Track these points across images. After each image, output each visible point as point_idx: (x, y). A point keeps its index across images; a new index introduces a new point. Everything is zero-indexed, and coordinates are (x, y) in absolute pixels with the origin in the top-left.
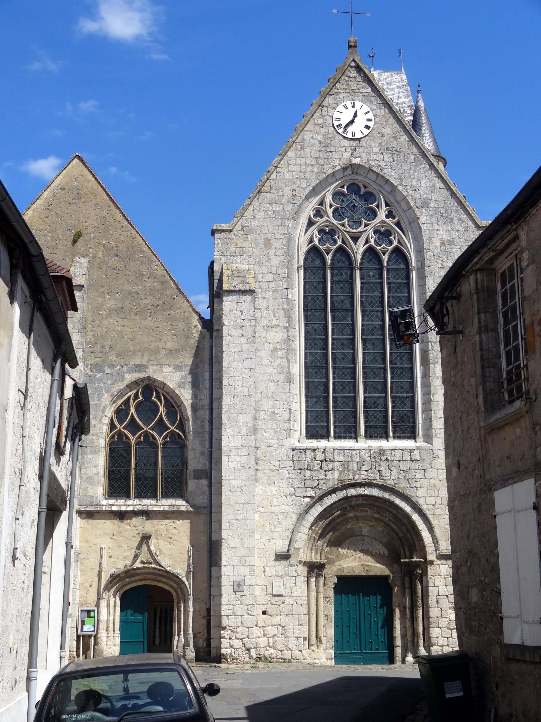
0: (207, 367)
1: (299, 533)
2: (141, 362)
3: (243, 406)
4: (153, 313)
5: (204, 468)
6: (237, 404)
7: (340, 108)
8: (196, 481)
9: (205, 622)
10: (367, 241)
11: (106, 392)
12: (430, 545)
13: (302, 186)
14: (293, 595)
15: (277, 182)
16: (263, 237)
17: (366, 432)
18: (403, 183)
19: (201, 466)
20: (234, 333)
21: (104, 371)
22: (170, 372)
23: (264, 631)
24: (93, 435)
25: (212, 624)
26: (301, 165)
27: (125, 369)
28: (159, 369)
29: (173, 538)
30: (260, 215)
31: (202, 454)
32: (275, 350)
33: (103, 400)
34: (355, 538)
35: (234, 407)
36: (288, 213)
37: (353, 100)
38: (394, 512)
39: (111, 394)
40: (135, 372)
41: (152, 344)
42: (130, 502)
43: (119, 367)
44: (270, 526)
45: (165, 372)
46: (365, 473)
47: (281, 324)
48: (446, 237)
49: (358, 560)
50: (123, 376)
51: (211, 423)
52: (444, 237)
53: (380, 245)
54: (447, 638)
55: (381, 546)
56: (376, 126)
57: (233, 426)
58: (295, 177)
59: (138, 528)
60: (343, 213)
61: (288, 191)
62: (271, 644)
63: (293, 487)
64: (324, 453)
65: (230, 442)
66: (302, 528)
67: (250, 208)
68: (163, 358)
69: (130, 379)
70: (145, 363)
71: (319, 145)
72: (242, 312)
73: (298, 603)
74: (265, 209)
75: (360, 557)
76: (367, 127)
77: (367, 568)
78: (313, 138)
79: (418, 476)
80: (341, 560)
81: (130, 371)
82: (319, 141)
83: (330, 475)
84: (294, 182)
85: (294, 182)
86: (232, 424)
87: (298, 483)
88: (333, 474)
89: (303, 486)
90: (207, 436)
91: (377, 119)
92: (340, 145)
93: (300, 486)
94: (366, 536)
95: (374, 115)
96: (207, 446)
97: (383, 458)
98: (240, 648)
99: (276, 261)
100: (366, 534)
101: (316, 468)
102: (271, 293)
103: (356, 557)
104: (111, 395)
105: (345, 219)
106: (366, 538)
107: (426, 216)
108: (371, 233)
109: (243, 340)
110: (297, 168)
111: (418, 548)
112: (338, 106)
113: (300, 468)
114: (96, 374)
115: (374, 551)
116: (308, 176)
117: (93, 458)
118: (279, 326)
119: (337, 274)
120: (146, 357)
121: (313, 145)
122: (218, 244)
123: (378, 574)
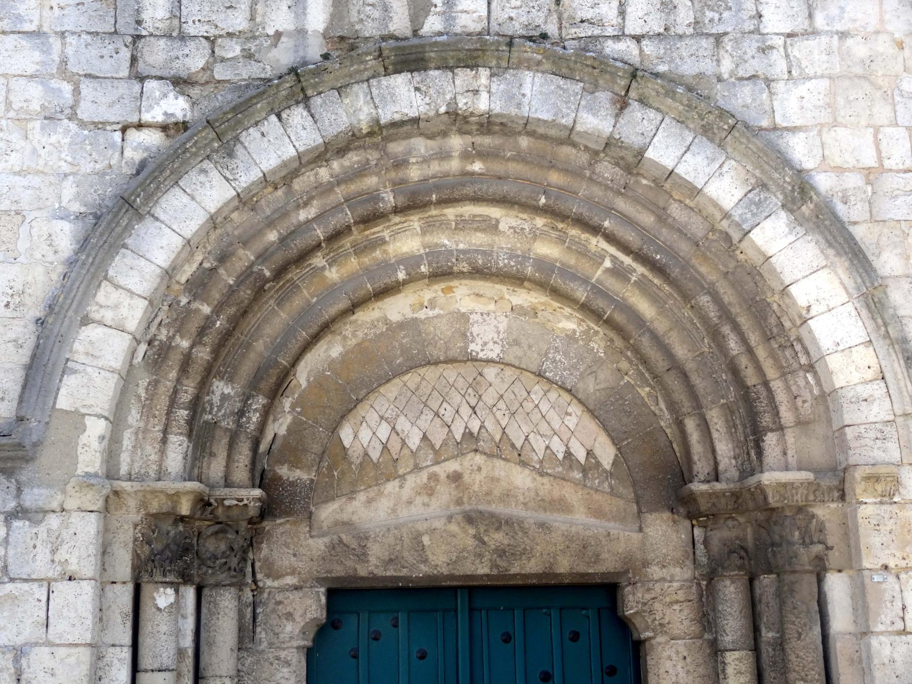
1: (86, 321)
34: (430, 373)
38: (647, 219)
49: (445, 493)
55: (576, 416)
66: (105, 294)
75: (456, 477)
77: (497, 538)
80: (351, 495)
87: (94, 52)
93: (105, 68)
94: (489, 361)
100: (493, 352)
103: (434, 477)
106: (490, 372)
111: (787, 416)
115: (539, 444)
123: (564, 566)
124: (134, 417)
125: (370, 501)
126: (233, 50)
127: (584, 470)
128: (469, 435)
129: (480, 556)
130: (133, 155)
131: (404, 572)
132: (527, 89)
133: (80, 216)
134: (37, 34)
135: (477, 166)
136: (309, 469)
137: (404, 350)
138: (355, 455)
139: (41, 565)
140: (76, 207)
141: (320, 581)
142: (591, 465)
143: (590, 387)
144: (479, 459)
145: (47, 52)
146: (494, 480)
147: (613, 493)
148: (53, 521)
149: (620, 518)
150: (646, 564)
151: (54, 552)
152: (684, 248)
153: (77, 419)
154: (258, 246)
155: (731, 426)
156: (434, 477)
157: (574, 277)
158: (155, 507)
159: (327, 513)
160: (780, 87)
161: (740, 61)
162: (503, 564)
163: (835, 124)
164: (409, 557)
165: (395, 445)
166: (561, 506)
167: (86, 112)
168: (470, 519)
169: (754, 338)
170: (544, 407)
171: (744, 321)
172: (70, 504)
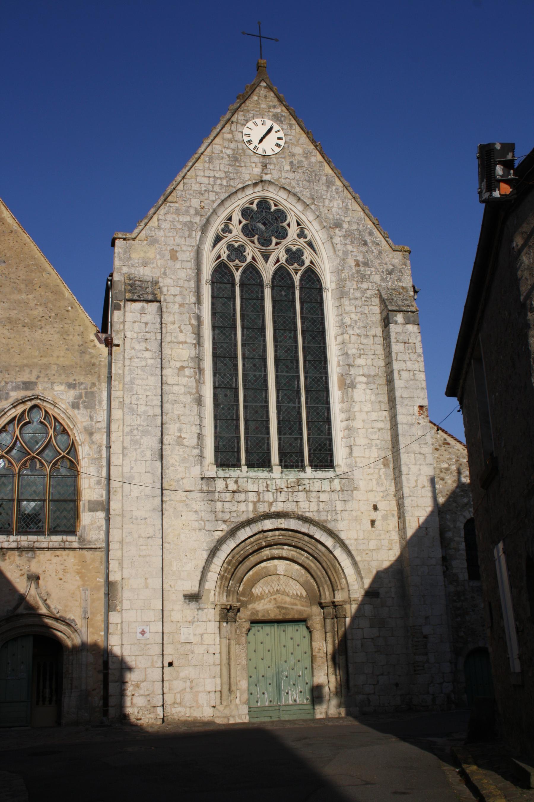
0: (104, 386)
1: (209, 571)
2: (29, 378)
3: (147, 427)
4: (43, 325)
5: (100, 499)
6: (140, 425)
7: (250, 124)
8: (92, 513)
9: (101, 677)
10: (278, 261)
12: (353, 583)
13: (211, 199)
14: (204, 643)
15: (183, 193)
16: (169, 248)
17: (281, 461)
18: (316, 203)
19: (97, 496)
20: (137, 347)
23: (169, 684)
25: (111, 678)
26: (209, 177)
27: (9, 386)
29: (64, 580)
30: (164, 225)
31: (99, 483)
32: (182, 368)
34: (269, 577)
35: (137, 429)
36: (196, 225)
37: (263, 118)
41: (41, 358)
42: (12, 538)
44: (176, 565)
45: (57, 391)
46: (282, 504)
47: (189, 341)
48: (360, 258)
49: (273, 602)
50: (7, 394)
51: (109, 447)
52: (358, 258)
53: (292, 265)
54: (374, 685)
56: (286, 145)
57: (136, 450)
58: (203, 189)
59: (22, 568)
60: (253, 230)
61: (196, 203)
62: (178, 701)
63: (202, 520)
64: (236, 482)
65: (132, 468)
67: (155, 218)
68: (54, 375)
69: (16, 397)
70: (33, 379)
71: (228, 159)
72: (146, 324)
73: (210, 652)
74: (171, 219)
75: (275, 599)
76: (278, 145)
77: (283, 611)
78: (222, 152)
79: (339, 508)
80: (255, 603)
81: (16, 388)
82: (228, 156)
83: (242, 507)
84: (202, 194)
85: (202, 194)
86: (134, 447)
88: (247, 506)
89: (214, 519)
90: (104, 463)
91: (289, 138)
92: (250, 160)
93: (210, 519)
95: (285, 135)
96: (104, 474)
97: (301, 488)
98: (145, 707)
99: (182, 274)
101: (227, 500)
102: (177, 306)
103: (271, 599)
105: (254, 236)
106: (282, 577)
107: (340, 237)
108: (283, 252)
109: (147, 354)
110: (206, 181)
111: (339, 587)
112: (247, 123)
113: (210, 499)
115: (291, 592)
116: (217, 189)
118: (186, 342)
119: (247, 292)
120: (35, 373)
121: (222, 158)
122: (119, 253)
124: (218, 589)
125: (258, 604)
126: (234, 514)
127: (300, 597)
128: (277, 590)
129: (280, 615)
130: (217, 537)
131: (266, 618)
132: (291, 523)
133: (207, 550)
134: (196, 511)
135: (281, 537)
136: (246, 597)
137: (265, 573)
138: (255, 595)
139: (204, 619)
140: (206, 548)
141: (250, 620)
142: (301, 596)
143: (301, 580)
144: (279, 595)
145: (198, 515)
146: (282, 599)
147: (305, 602)
148: (206, 610)
149: (307, 607)
150: (312, 616)
151: (207, 616)
152: (320, 554)
153: (209, 591)
154: (239, 554)
155: (328, 589)
156: (271, 599)
157: (299, 558)
158: (223, 607)
159: (250, 606)
160: (339, 522)
161: (332, 517)
162: (284, 616)
163: (350, 530)
164: (266, 615)
165: (263, 593)
166: (295, 604)
167: (207, 528)
168: (278, 607)
169: (333, 572)
170: (292, 584)
171: (332, 569)
172: (209, 607)
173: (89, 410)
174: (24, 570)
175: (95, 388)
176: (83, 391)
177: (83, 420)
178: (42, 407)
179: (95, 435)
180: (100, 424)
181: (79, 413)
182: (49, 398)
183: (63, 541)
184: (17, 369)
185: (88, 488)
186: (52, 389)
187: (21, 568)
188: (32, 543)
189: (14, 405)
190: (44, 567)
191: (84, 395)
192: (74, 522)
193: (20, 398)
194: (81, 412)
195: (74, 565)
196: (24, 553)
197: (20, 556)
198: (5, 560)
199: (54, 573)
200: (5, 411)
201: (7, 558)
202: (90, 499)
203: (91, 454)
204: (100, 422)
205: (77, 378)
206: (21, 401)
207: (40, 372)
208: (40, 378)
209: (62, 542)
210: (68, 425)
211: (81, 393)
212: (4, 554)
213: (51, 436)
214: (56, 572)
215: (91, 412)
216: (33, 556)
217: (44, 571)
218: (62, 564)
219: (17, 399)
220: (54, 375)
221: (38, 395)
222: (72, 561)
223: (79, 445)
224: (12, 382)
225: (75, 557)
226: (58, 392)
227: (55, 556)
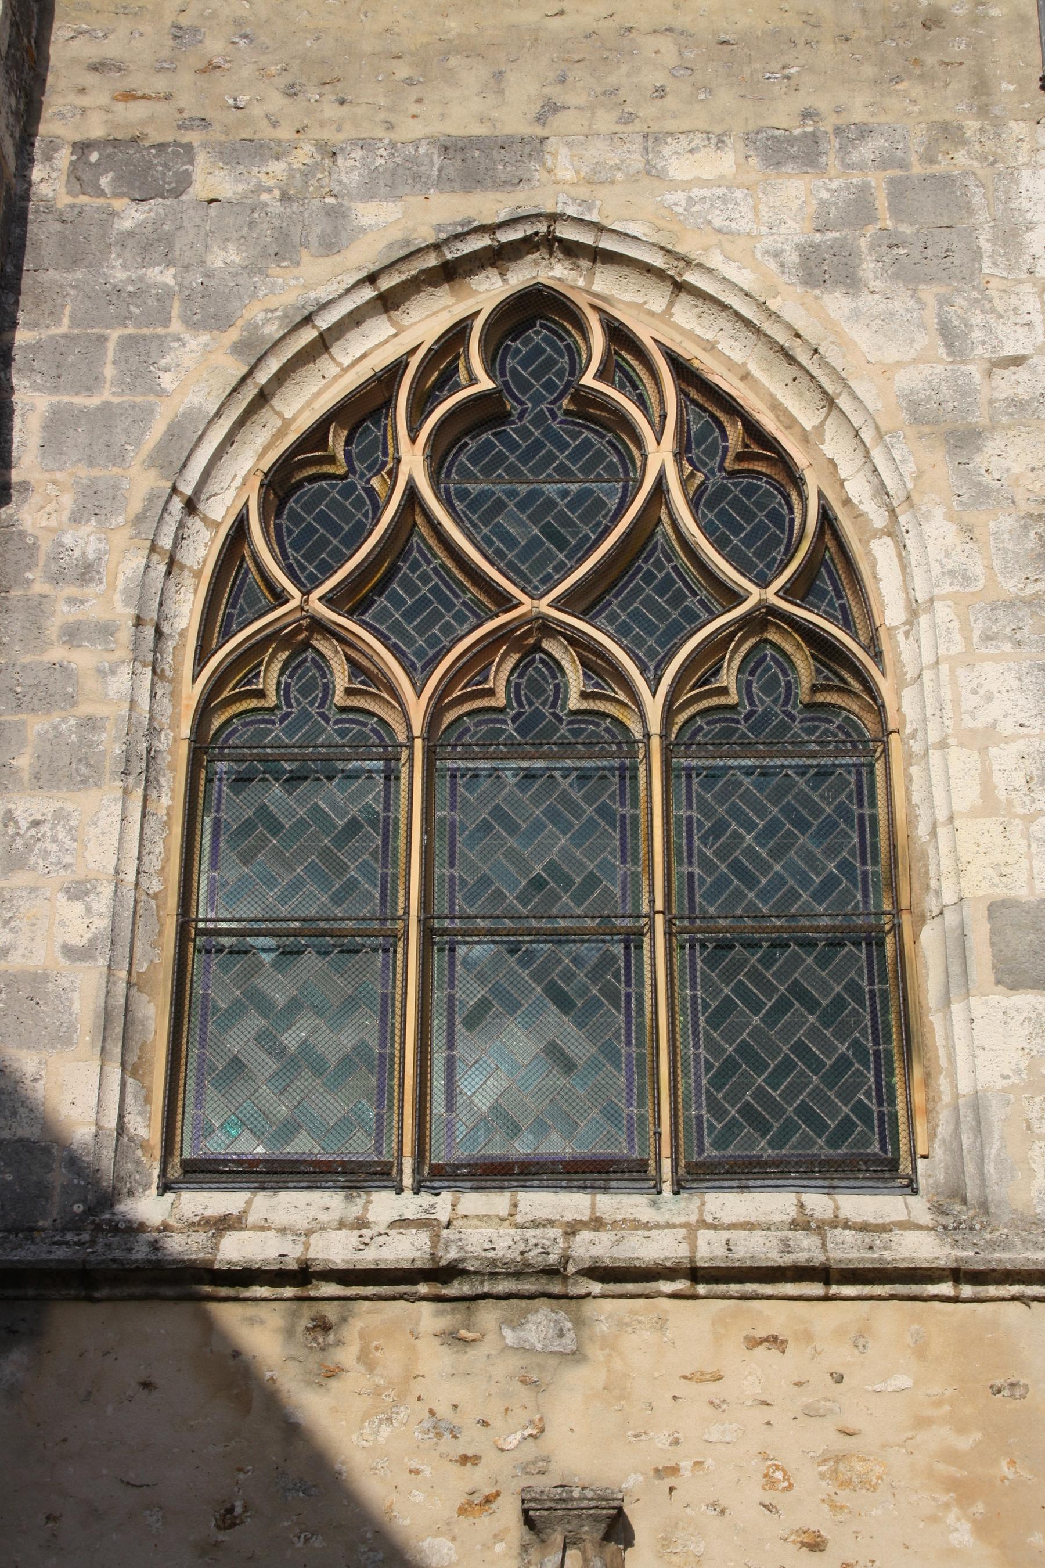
11: (192, 325)
21: (185, 181)
22: (719, 181)
24: (72, 635)
28: (636, 161)
33: (167, 380)
39: (233, 335)
40: (443, 182)
43: (305, 154)
45: (685, 186)
50: (337, 214)
59: (472, 1441)
68: (660, 92)
104: (238, 348)
114: (118, 204)
117: (59, 815)
173: (928, 293)
174: (491, 1460)
175: (961, 157)
176: (878, 181)
177: (892, 355)
178: (582, 301)
179: (992, 446)
180: (1022, 373)
181: (856, 313)
182: (633, 229)
183: (802, 1224)
184: (403, 71)
185: (974, 813)
186: (653, 172)
187: (463, 1447)
188: (556, 1232)
189: (386, 283)
190: (662, 1440)
191: (882, 202)
192: (885, 1095)
193: (426, 236)
194: (867, 301)
195: (922, 1423)
196: (488, 1315)
197: (453, 1339)
198: (333, 1373)
199: (758, 1493)
200: (325, 321)
201: (347, 1355)
202: (1000, 892)
203: (978, 569)
204: (1018, 361)
205: (822, 104)
206: (432, 261)
207: (563, 80)
208: (562, 115)
209: (794, 1225)
210: (776, 407)
211: (864, 189)
212: (323, 1326)
213: (661, 479)
214: (770, 1482)
215: (944, 301)
216: (569, 1343)
217: (660, 1473)
218: (811, 1413)
219: (407, 242)
220: (660, 92)
221: (554, 217)
222: (903, 1381)
223: (870, 534)
224: (365, 144)
225: (921, 1351)
226: (696, 192)
227: (753, 1343)
